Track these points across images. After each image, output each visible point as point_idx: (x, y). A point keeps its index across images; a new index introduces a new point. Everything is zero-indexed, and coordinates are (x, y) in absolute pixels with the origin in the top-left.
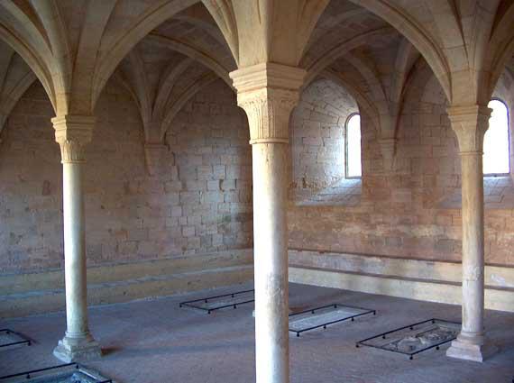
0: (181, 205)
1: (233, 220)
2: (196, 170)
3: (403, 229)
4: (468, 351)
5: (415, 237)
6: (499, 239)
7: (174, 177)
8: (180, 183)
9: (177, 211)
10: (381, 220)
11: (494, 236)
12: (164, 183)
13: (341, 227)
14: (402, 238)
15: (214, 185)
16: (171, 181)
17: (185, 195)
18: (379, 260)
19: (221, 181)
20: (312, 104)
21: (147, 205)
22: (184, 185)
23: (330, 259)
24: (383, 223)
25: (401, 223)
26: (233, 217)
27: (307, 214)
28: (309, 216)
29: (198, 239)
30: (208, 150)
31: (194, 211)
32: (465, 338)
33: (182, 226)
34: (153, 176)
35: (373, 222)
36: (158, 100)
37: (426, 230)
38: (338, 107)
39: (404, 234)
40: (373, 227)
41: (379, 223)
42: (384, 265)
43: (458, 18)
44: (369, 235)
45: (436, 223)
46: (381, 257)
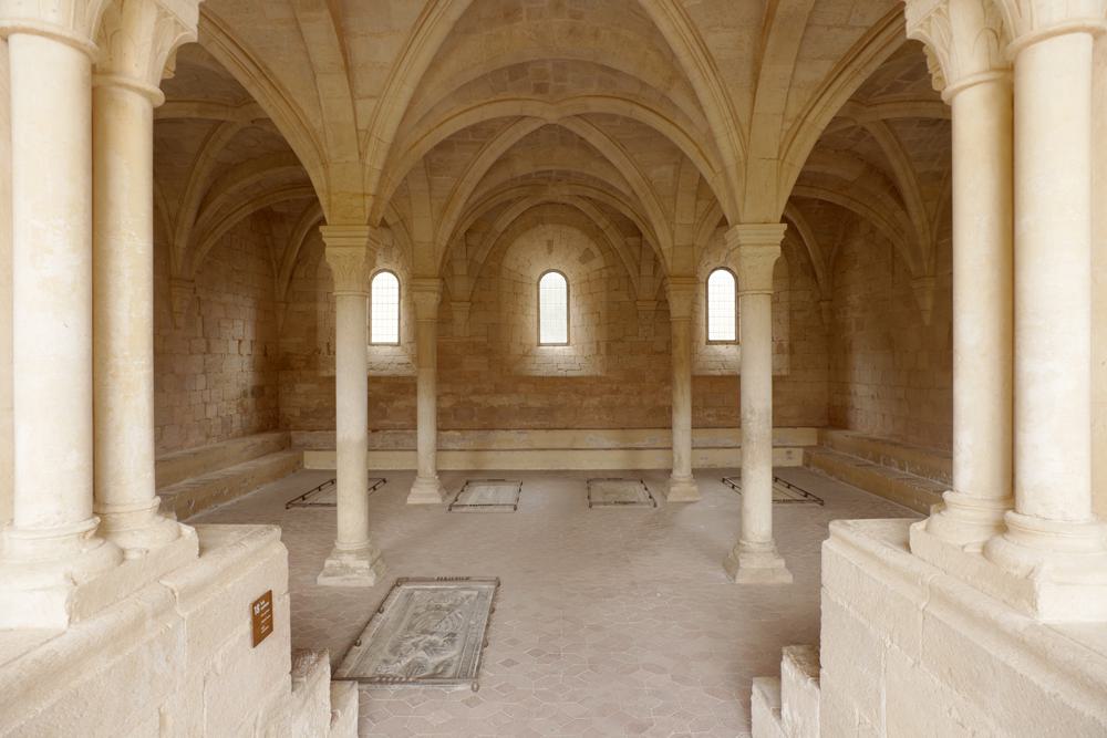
0: (204, 372)
1: (249, 395)
2: (219, 323)
3: (475, 399)
6: (585, 403)
7: (200, 334)
8: (204, 341)
9: (201, 382)
10: (448, 390)
11: (579, 402)
12: (189, 341)
13: (391, 400)
15: (233, 346)
16: (196, 338)
17: (210, 360)
18: (457, 434)
19: (240, 342)
21: (173, 372)
22: (208, 344)
23: (387, 437)
24: (453, 394)
25: (475, 392)
26: (249, 391)
29: (220, 420)
30: (229, 298)
31: (217, 382)
33: (206, 403)
34: (179, 328)
36: (200, 221)
37: (504, 398)
39: (478, 404)
42: (464, 439)
43: (698, 199)
45: (515, 392)
46: (460, 430)
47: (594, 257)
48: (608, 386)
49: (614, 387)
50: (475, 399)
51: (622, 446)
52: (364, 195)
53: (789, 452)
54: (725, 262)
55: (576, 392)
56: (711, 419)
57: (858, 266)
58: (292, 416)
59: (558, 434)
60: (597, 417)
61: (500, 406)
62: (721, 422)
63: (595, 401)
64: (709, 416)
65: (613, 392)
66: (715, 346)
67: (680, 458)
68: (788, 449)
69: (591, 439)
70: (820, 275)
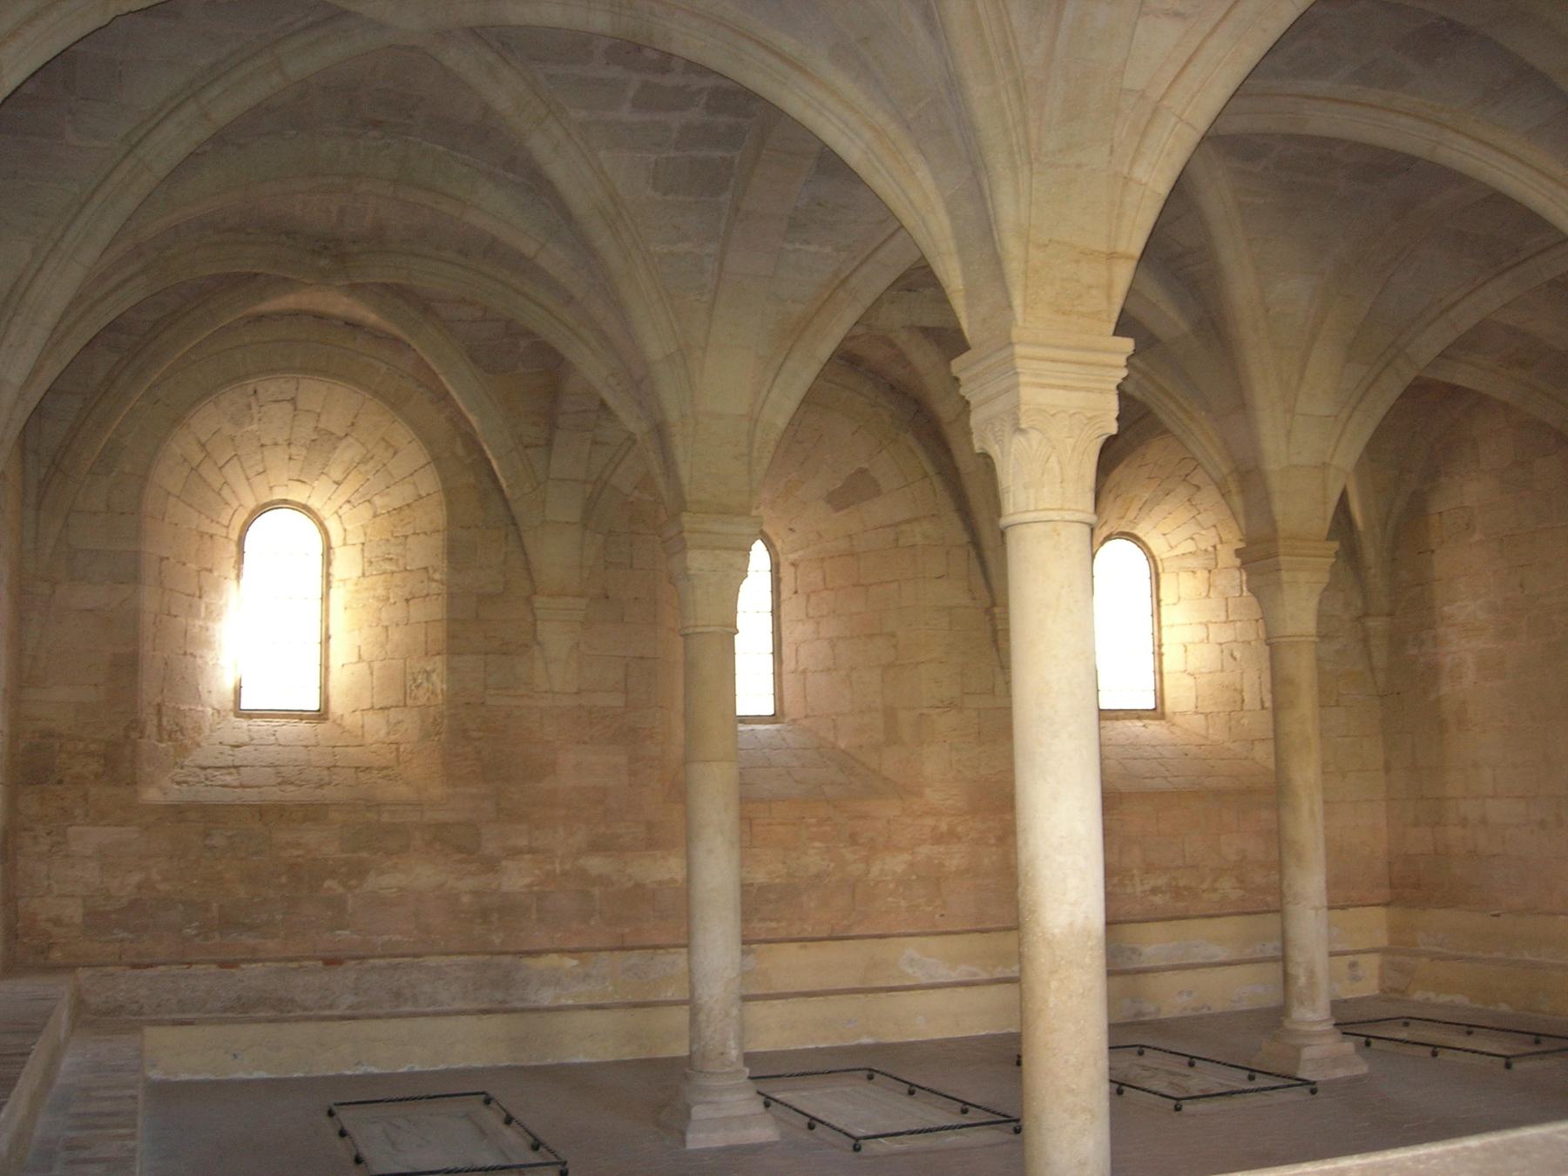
3: (596, 864)
4: (1336, 1061)
5: (638, 885)
6: (875, 870)
10: (522, 842)
11: (862, 866)
13: (359, 871)
14: (596, 891)
18: (570, 963)
20: (203, 446)
24: (532, 851)
25: (595, 847)
27: (207, 835)
28: (218, 840)
32: (1322, 1034)
35: (490, 847)
38: (251, 473)
40: (491, 865)
41: (515, 853)
42: (586, 977)
44: (475, 893)
47: (878, 493)
48: (930, 821)
49: (944, 827)
50: (596, 864)
51: (984, 976)
52: (1112, 256)
53: (1353, 965)
54: (1134, 522)
55: (853, 839)
56: (1158, 899)
57: (1476, 537)
58: (57, 922)
59: (833, 951)
60: (903, 903)
61: (660, 883)
62: (1181, 904)
63: (896, 864)
64: (1154, 891)
65: (938, 839)
66: (1119, 724)
67: (1311, 974)
68: (1351, 958)
69: (911, 961)
70: (1370, 554)
